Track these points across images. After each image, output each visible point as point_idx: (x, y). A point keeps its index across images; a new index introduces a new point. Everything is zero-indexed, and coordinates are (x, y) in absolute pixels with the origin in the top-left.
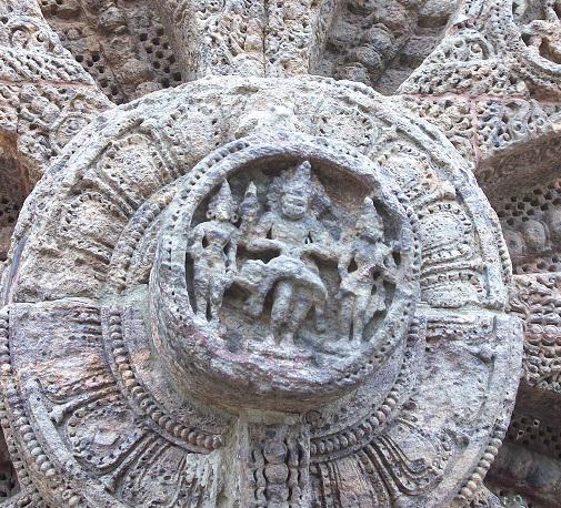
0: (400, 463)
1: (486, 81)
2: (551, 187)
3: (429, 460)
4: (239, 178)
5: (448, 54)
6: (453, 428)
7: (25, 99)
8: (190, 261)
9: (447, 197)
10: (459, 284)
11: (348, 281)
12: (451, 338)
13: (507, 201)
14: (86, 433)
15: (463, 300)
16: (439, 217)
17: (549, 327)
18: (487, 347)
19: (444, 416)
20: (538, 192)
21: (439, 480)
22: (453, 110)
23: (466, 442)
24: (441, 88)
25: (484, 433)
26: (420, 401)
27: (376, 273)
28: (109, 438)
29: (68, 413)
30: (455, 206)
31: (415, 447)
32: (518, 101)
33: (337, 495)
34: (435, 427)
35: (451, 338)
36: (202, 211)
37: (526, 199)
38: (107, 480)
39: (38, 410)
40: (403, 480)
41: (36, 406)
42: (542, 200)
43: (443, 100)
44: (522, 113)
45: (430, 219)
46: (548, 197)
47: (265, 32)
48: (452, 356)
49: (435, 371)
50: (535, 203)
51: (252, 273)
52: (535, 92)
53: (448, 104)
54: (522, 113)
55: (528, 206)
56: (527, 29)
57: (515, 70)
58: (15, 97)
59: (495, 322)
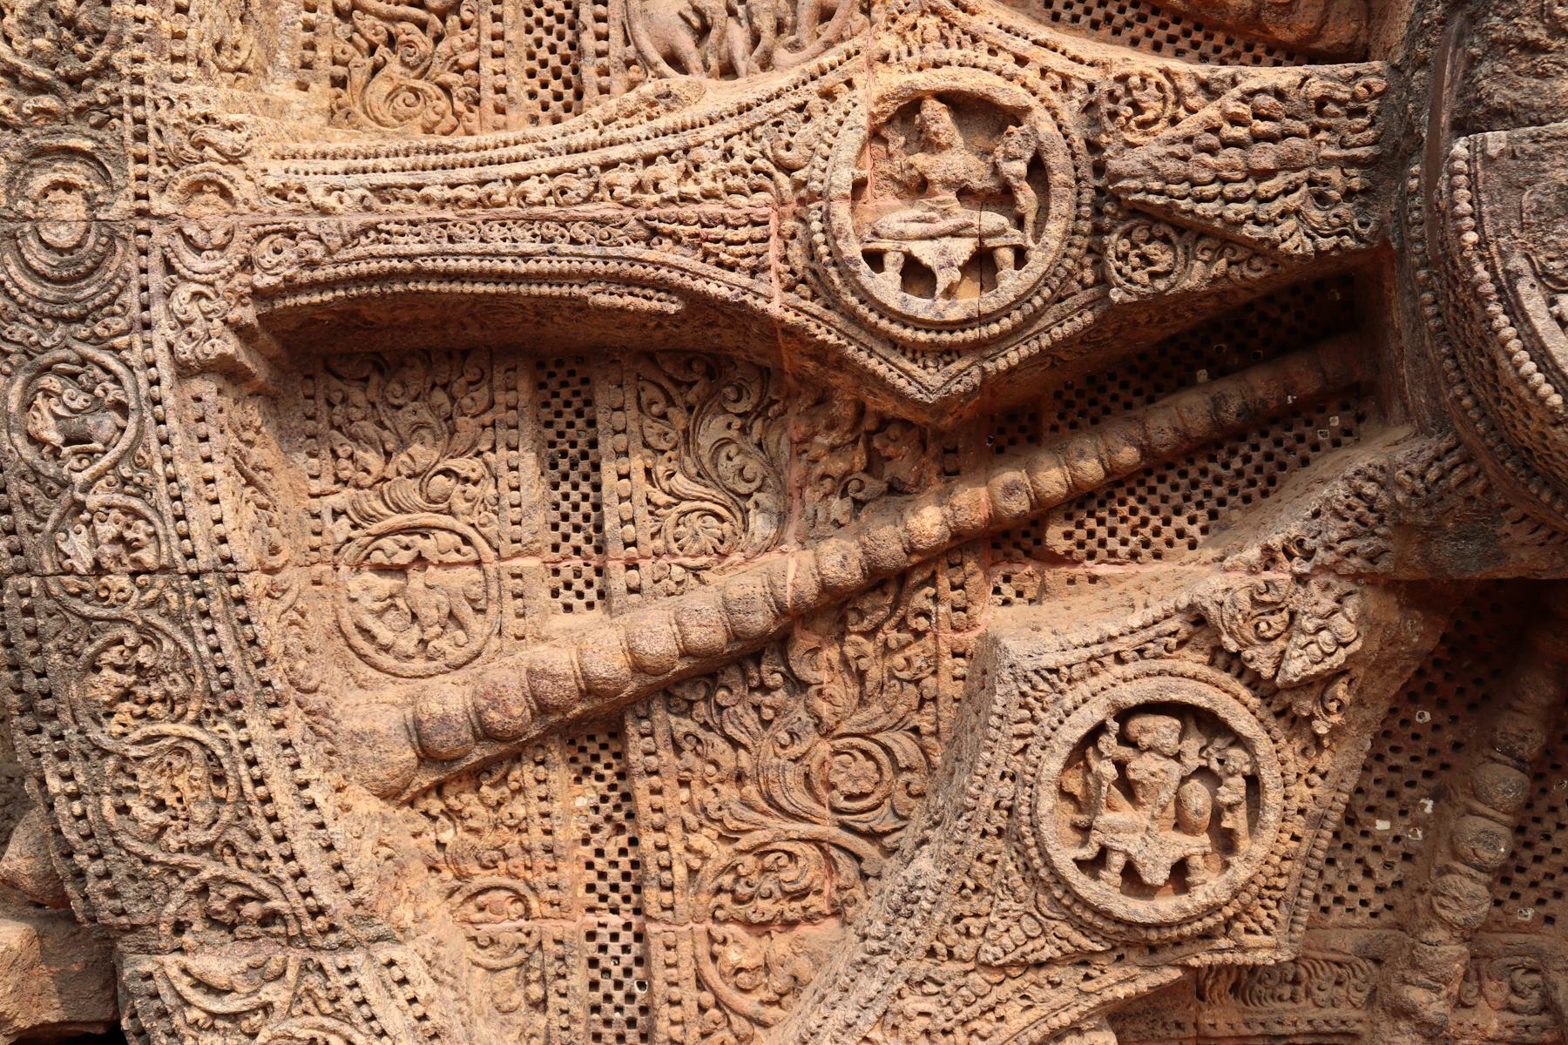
41: (1529, 296)
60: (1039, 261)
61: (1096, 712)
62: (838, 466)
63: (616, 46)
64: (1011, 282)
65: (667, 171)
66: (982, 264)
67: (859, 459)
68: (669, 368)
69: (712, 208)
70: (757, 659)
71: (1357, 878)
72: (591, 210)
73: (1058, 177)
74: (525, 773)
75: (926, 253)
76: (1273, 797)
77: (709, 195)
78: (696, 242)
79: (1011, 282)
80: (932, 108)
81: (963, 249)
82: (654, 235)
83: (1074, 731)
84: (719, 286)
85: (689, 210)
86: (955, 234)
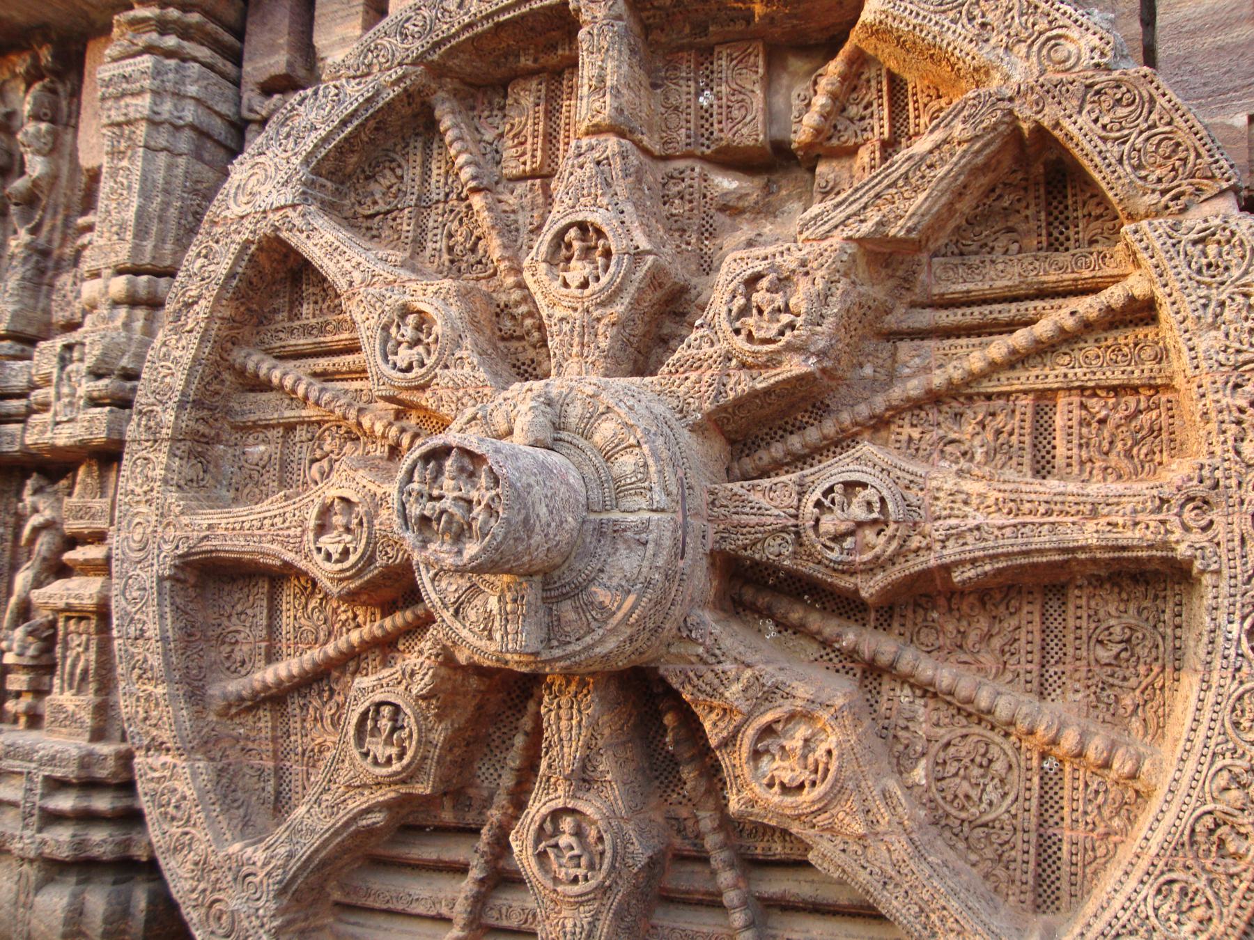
0: (592, 603)
1: (710, 361)
2: (796, 419)
3: (607, 602)
4: (427, 457)
5: (689, 346)
6: (623, 583)
7: (458, 399)
8: (403, 505)
9: (631, 446)
10: (636, 498)
11: (477, 510)
12: (624, 530)
13: (765, 430)
14: (444, 584)
15: (636, 507)
16: (625, 458)
17: (744, 517)
18: (644, 535)
19: (620, 575)
20: (787, 423)
21: (614, 613)
22: (688, 383)
23: (629, 592)
24: (681, 370)
25: (639, 586)
26: (607, 568)
27: (488, 506)
28: (454, 587)
29: (436, 574)
30: (637, 450)
31: (601, 594)
32: (732, 372)
33: (559, 620)
34: (615, 582)
35: (624, 530)
36: (409, 478)
37: (780, 428)
38: (451, 610)
39: (423, 572)
40: (594, 613)
42: (789, 428)
43: (683, 376)
44: (733, 380)
45: (621, 459)
46: (793, 426)
47: (583, 345)
48: (626, 541)
49: (617, 550)
50: (785, 430)
51: (429, 509)
52: (743, 365)
53: (687, 378)
54: (733, 380)
55: (780, 432)
56: (738, 325)
57: (728, 351)
58: (454, 399)
59: (649, 521)
60: (360, 551)
61: (367, 704)
62: (343, 617)
63: (301, 478)
64: (353, 558)
65: (278, 520)
66: (345, 553)
67: (350, 614)
68: (303, 582)
69: (286, 533)
70: (322, 680)
71: (492, 771)
72: (261, 532)
73: (365, 525)
74: (261, 713)
75: (331, 549)
76: (415, 736)
77: (288, 528)
78: (282, 542)
79: (353, 558)
80: (336, 501)
81: (340, 547)
82: (273, 541)
83: (361, 709)
84: (289, 556)
85: (280, 533)
86: (339, 542)
